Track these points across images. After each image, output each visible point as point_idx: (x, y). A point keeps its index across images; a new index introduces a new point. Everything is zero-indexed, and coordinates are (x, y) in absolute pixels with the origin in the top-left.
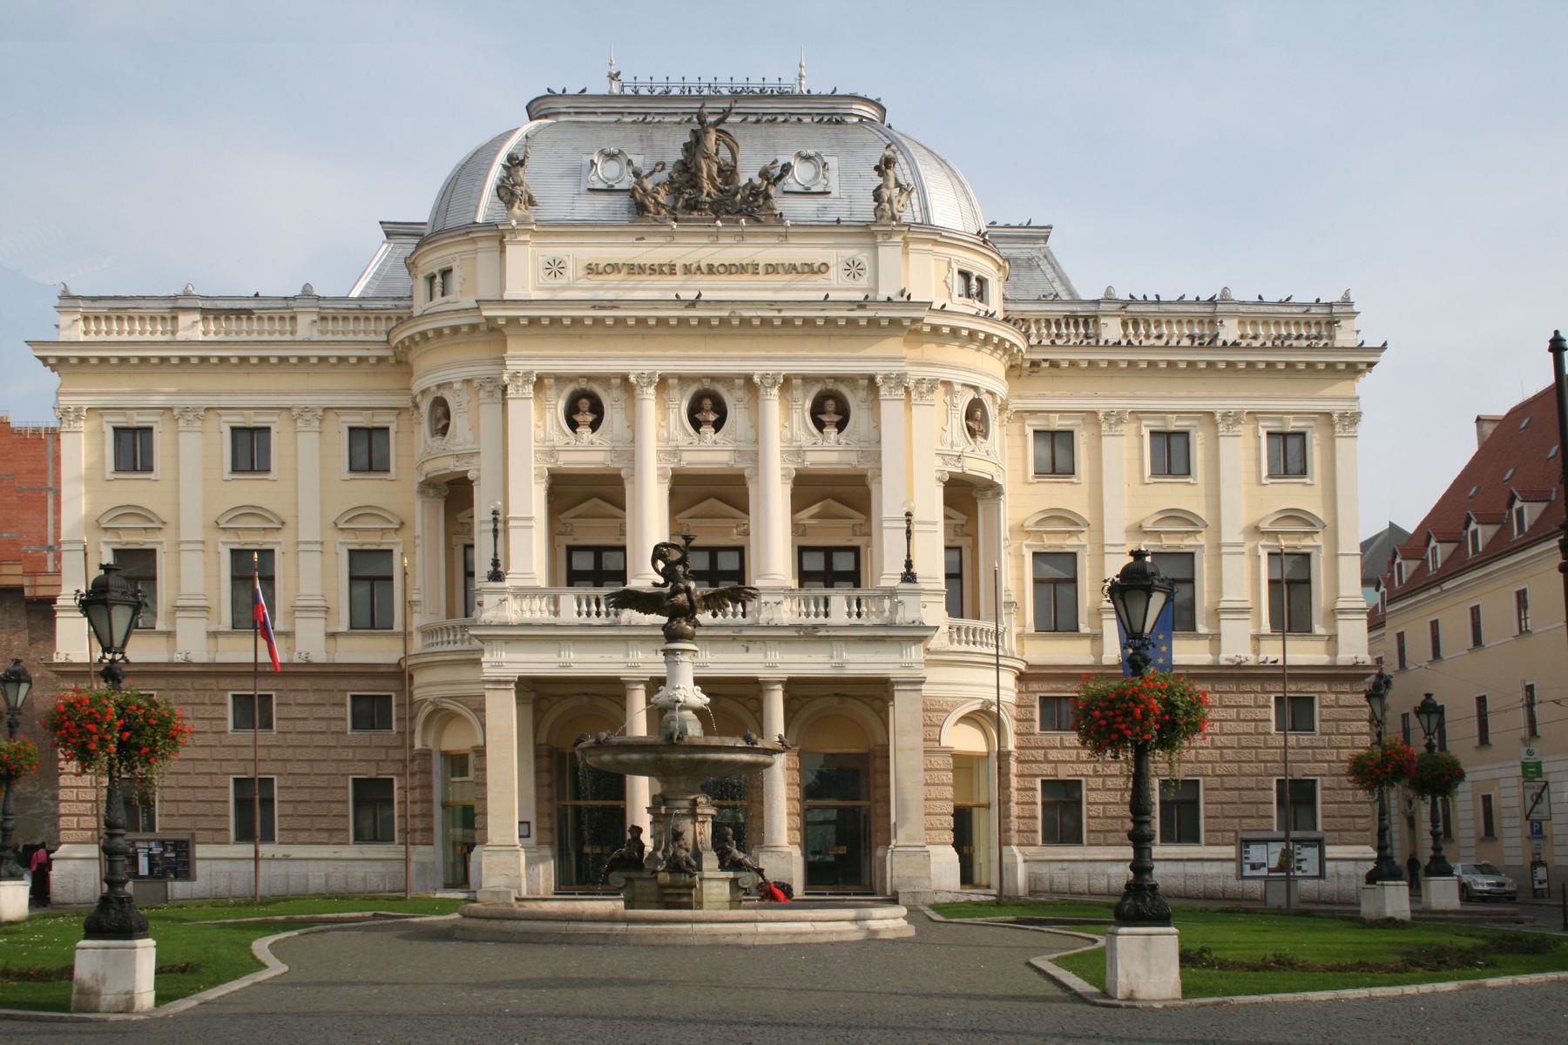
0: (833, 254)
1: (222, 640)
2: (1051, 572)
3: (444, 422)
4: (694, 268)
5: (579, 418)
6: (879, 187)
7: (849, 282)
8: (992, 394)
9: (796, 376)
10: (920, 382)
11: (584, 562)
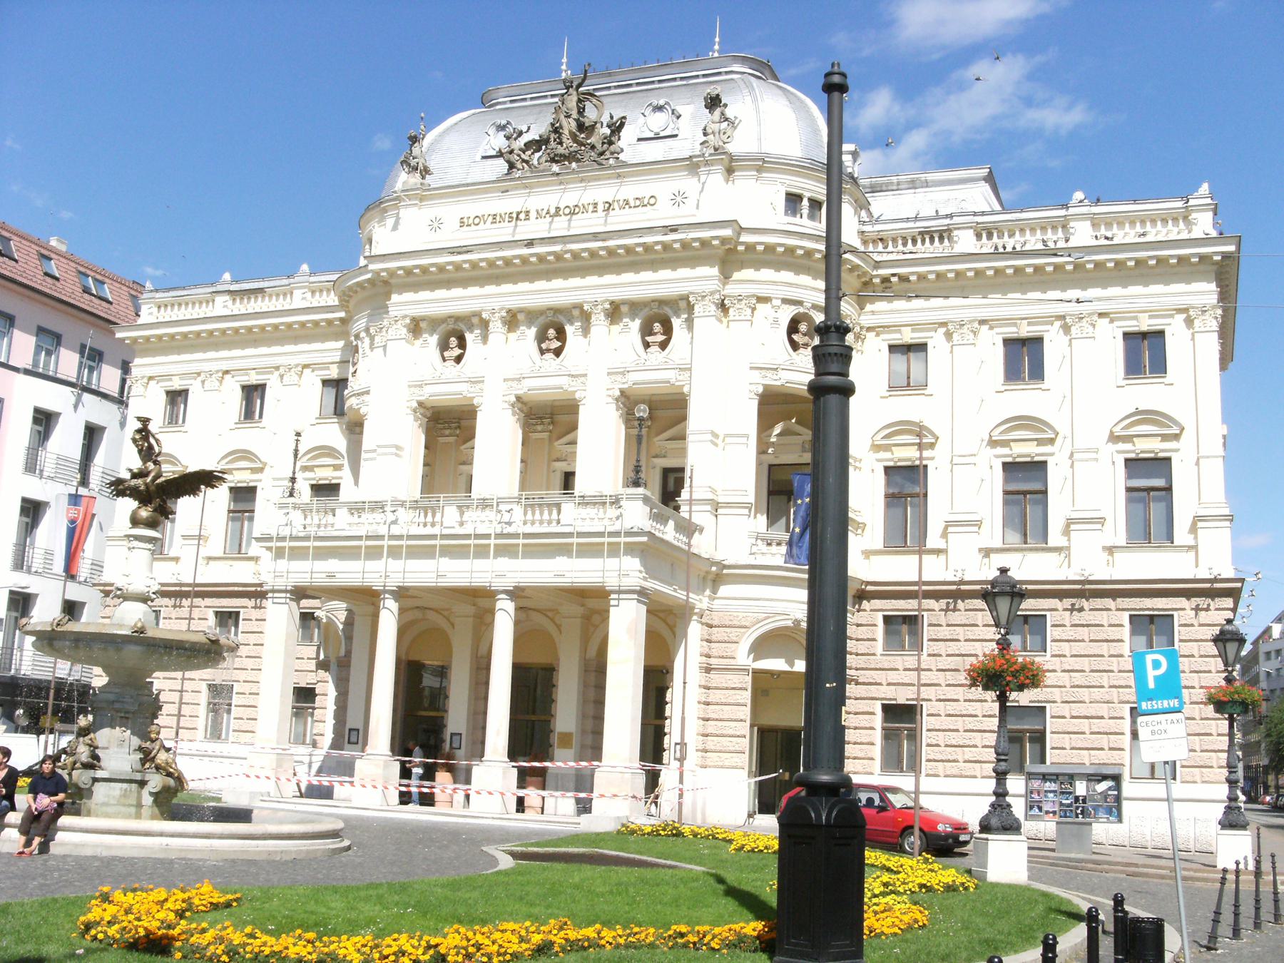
0: (662, 187)
9: (624, 302)
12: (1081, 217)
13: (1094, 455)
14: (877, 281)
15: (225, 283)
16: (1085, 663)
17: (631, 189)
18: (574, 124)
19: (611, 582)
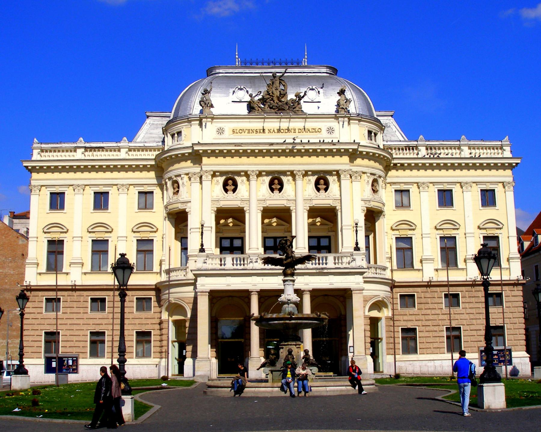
0: (324, 125)
1: (87, 275)
2: (403, 245)
3: (177, 189)
4: (272, 131)
5: (228, 187)
6: (339, 100)
7: (329, 135)
8: (380, 177)
10: (356, 172)
11: (226, 243)
12: (465, 145)
13: (472, 235)
14: (392, 165)
16: (473, 311)
17: (311, 124)
18: (279, 93)
19: (352, 286)
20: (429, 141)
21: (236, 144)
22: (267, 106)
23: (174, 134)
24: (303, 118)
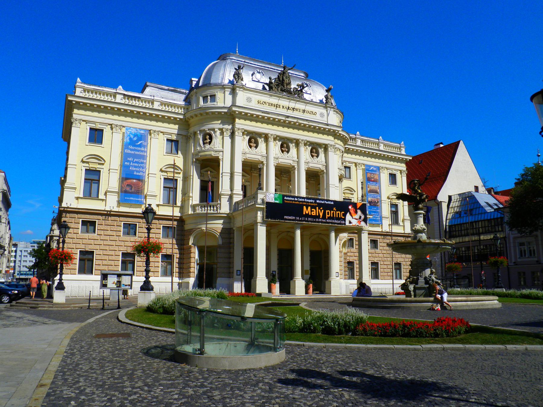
5: (252, 144)
7: (321, 118)
15: (120, 89)
17: (309, 108)
20: (362, 136)
21: (263, 112)
22: (279, 89)
23: (207, 96)
24: (305, 103)
